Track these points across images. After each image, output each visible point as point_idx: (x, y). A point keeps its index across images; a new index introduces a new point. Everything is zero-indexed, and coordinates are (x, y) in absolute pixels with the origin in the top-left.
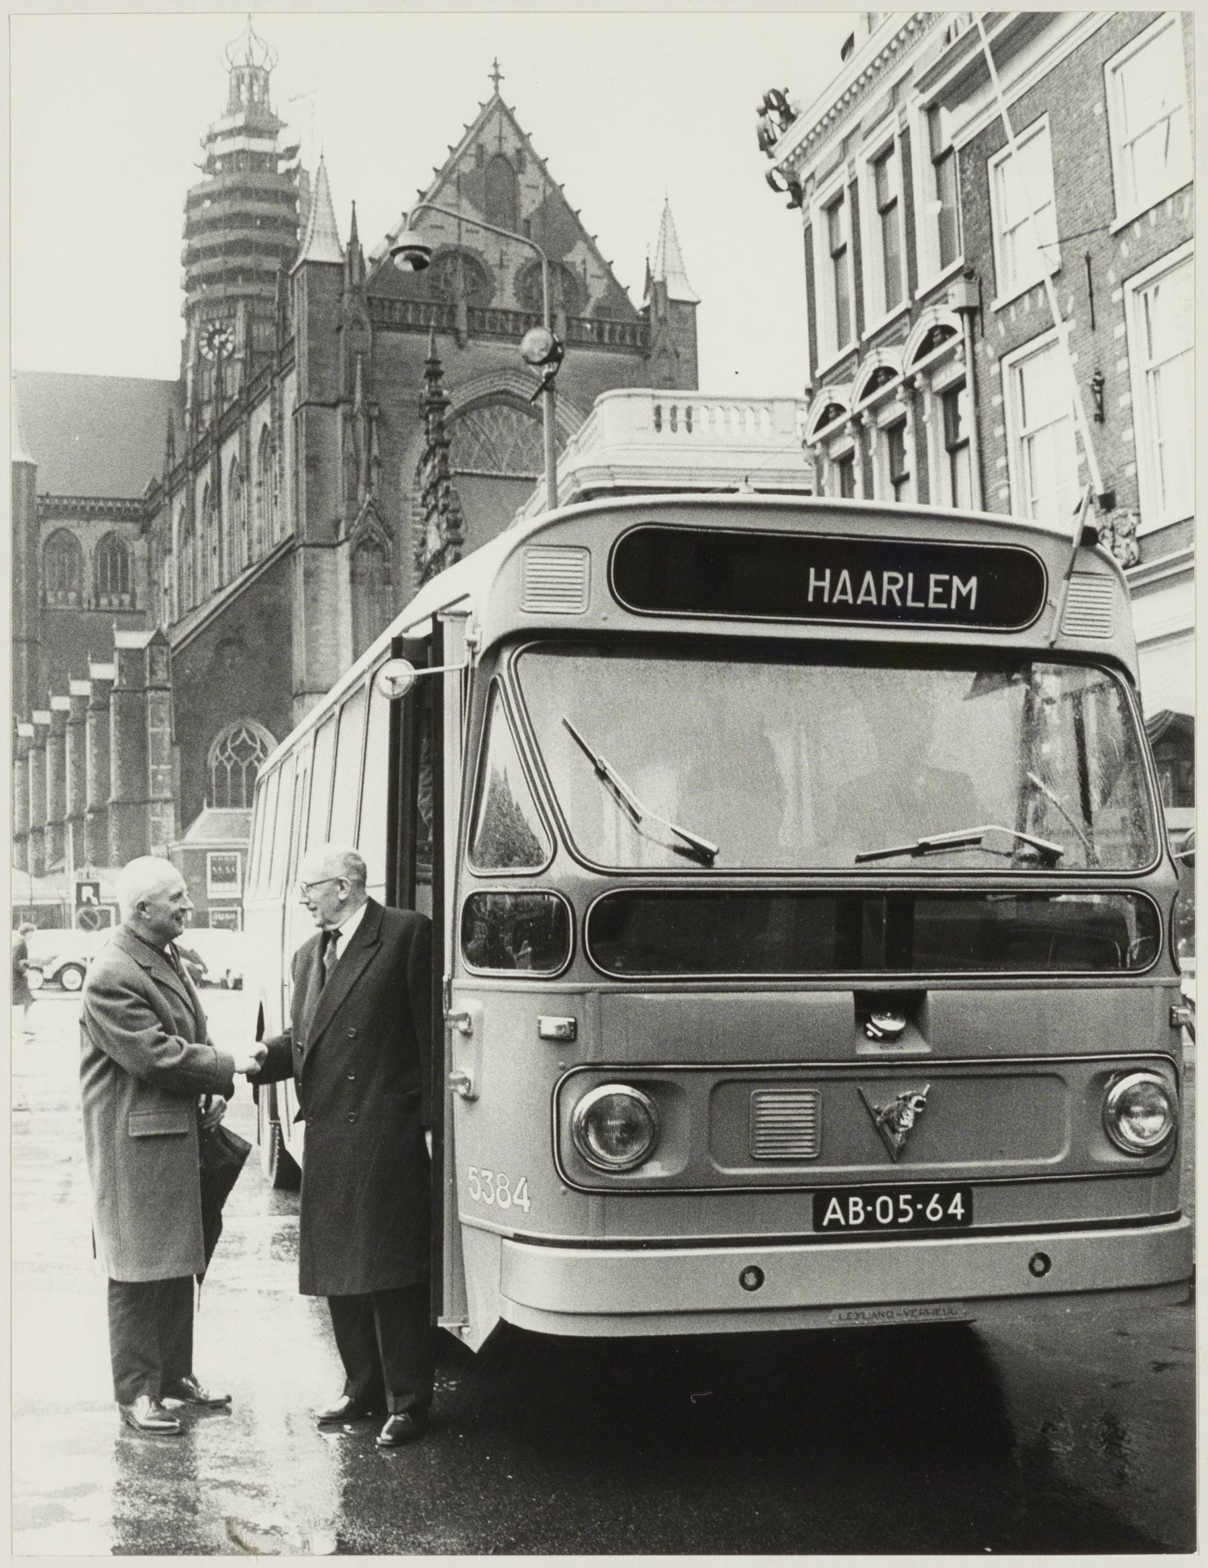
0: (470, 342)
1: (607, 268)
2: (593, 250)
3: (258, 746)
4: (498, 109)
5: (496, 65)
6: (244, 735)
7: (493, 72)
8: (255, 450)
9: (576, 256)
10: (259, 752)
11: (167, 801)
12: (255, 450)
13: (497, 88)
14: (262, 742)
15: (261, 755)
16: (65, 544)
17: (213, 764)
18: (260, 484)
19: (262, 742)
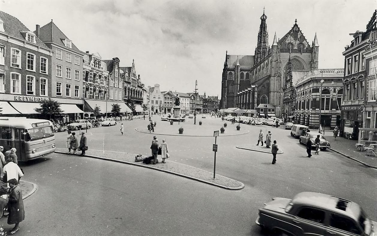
0: (291, 53)
2: (306, 41)
4: (296, 25)
5: (296, 20)
8: (265, 65)
12: (265, 65)
13: (296, 23)
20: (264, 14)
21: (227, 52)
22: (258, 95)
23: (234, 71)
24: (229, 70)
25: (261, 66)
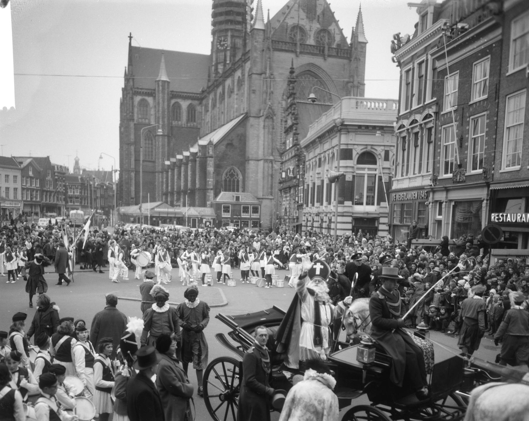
1: (341, 30)
2: (337, 25)
6: (232, 171)
9: (332, 28)
10: (236, 176)
11: (211, 189)
16: (177, 106)
17: (223, 179)
18: (237, 94)
22: (218, 167)
25: (227, 87)
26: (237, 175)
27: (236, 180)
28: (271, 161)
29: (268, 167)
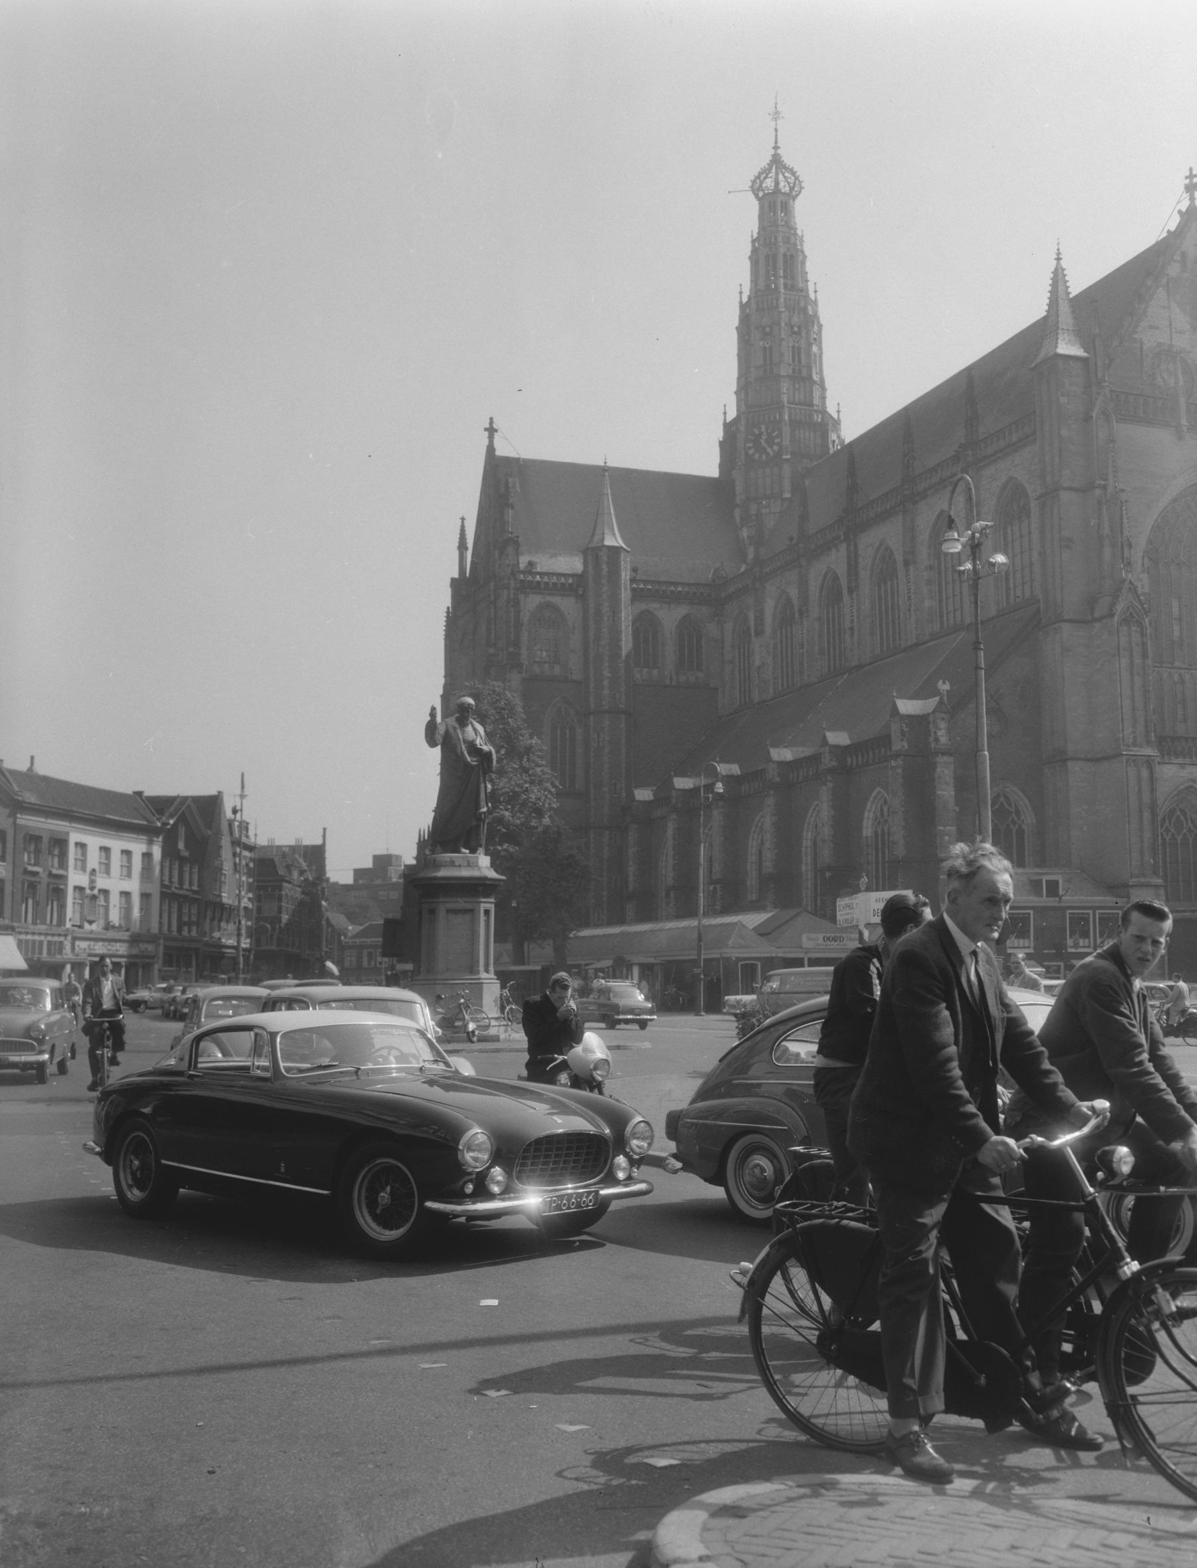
3: (1013, 810)
7: (1187, 181)
14: (1016, 807)
15: (1016, 819)
19: (1016, 807)
20: (776, 161)
21: (491, 431)
23: (582, 598)
24: (536, 588)
26: (1018, 813)
27: (1014, 829)
28: (1149, 762)
29: (1139, 779)
